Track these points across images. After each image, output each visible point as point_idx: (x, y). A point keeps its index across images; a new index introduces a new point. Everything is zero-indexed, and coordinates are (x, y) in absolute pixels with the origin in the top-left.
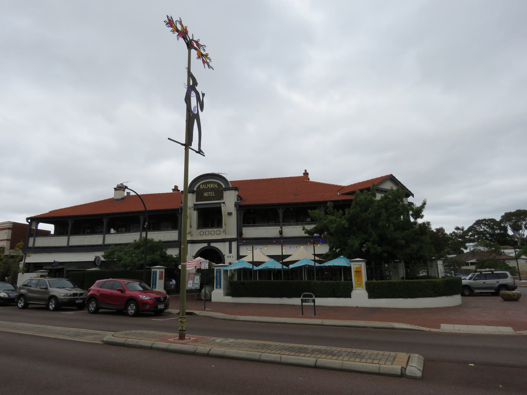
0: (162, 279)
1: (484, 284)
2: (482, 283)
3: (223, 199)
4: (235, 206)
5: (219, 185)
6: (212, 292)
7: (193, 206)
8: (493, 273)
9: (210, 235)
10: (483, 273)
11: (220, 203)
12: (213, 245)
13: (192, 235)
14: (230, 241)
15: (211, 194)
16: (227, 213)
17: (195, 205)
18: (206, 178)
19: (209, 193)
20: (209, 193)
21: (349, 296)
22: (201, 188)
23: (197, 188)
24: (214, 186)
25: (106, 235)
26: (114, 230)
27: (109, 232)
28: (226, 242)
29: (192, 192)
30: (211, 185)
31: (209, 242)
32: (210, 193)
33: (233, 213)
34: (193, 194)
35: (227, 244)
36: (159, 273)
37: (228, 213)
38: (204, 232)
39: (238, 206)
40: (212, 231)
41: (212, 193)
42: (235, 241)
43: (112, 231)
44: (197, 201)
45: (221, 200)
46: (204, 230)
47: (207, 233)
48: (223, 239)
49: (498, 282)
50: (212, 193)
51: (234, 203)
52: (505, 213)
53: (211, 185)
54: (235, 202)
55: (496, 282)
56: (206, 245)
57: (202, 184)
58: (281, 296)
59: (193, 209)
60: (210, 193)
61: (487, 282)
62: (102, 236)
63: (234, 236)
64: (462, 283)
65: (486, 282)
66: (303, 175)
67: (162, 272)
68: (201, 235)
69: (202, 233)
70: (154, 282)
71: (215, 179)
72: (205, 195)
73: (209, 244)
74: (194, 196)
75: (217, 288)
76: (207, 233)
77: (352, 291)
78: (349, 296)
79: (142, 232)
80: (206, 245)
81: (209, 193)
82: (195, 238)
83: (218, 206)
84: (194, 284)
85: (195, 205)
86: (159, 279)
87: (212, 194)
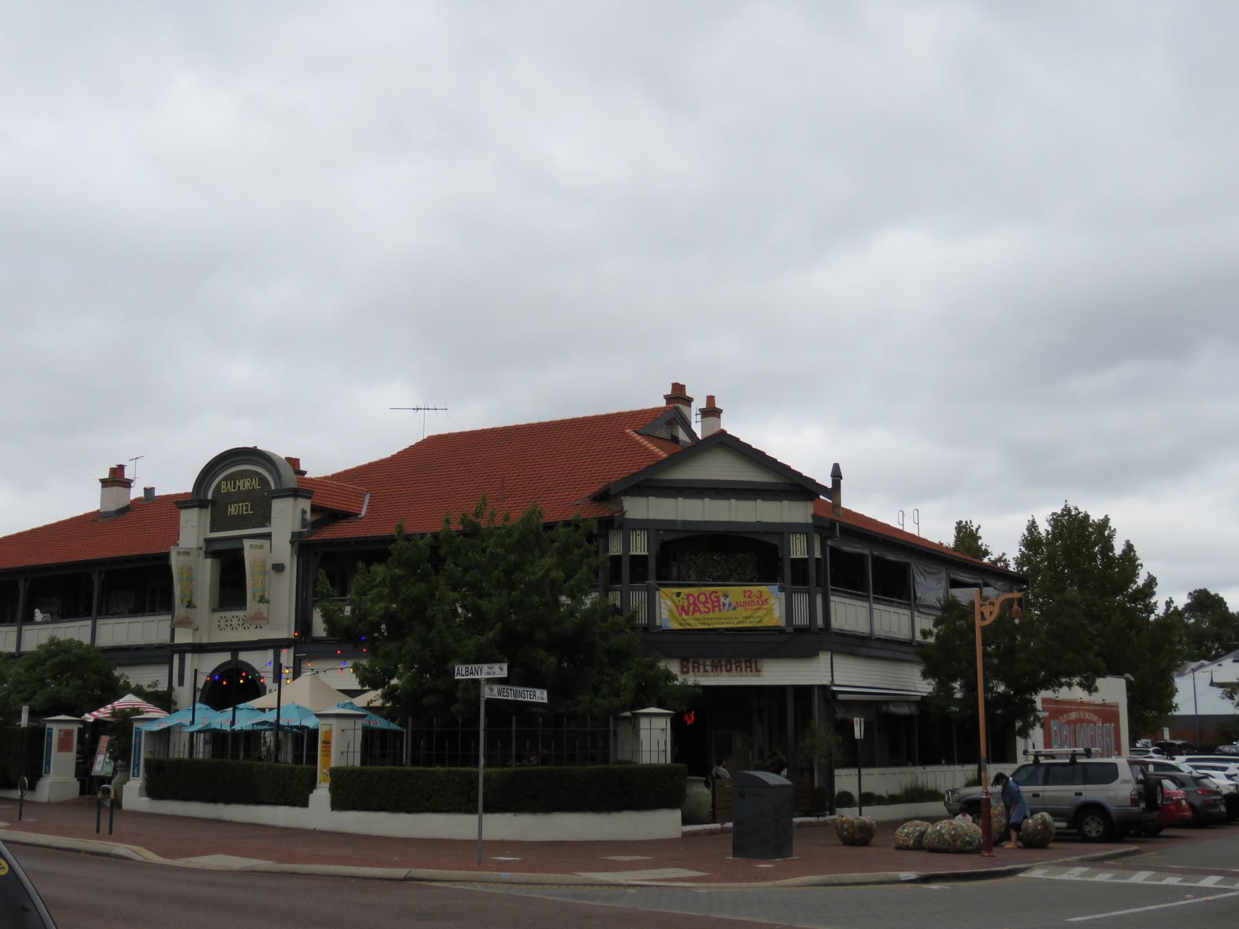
0: (69, 749)
1: (1077, 797)
2: (1031, 794)
3: (270, 523)
4: (292, 543)
5: (263, 481)
6: (124, 786)
7: (202, 544)
8: (1073, 762)
9: (240, 628)
10: (1079, 761)
11: (240, 538)
12: (244, 656)
13: (197, 630)
14: (277, 645)
15: (245, 508)
16: (269, 566)
17: (208, 541)
18: (234, 462)
19: (239, 506)
20: (240, 504)
21: (305, 804)
22: (223, 492)
23: (214, 491)
24: (251, 485)
25: (25, 628)
26: (42, 613)
27: (29, 619)
28: (269, 650)
29: (196, 504)
30: (244, 482)
31: (235, 648)
32: (242, 506)
33: (285, 564)
34: (204, 510)
35: (270, 654)
36: (60, 735)
37: (273, 565)
38: (238, 623)
39: (297, 544)
40: (233, 617)
41: (247, 506)
42: (288, 647)
43: (38, 615)
44: (212, 531)
45: (266, 526)
46: (229, 614)
47: (235, 622)
48: (260, 641)
49: (1080, 794)
50: (247, 506)
51: (289, 537)
52: (72, 637)
53: (244, 482)
54: (293, 534)
55: (1072, 794)
56: (226, 657)
57: (225, 479)
58: (214, 800)
59: (202, 553)
60: (242, 506)
61: (1046, 794)
62: (15, 629)
63: (286, 630)
64: (338, 765)
65: (1041, 794)
66: (662, 403)
67: (69, 733)
68: (221, 630)
69: (223, 623)
70: (136, 762)
71: (255, 465)
72: (231, 512)
73: (235, 656)
74: (207, 514)
75: (133, 776)
76: (235, 622)
77: (314, 791)
78: (305, 804)
79: (22, 624)
80: (226, 657)
81: (239, 506)
82: (204, 639)
83: (233, 545)
84: (105, 764)
85: (208, 541)
86: (56, 750)
87: (247, 510)
